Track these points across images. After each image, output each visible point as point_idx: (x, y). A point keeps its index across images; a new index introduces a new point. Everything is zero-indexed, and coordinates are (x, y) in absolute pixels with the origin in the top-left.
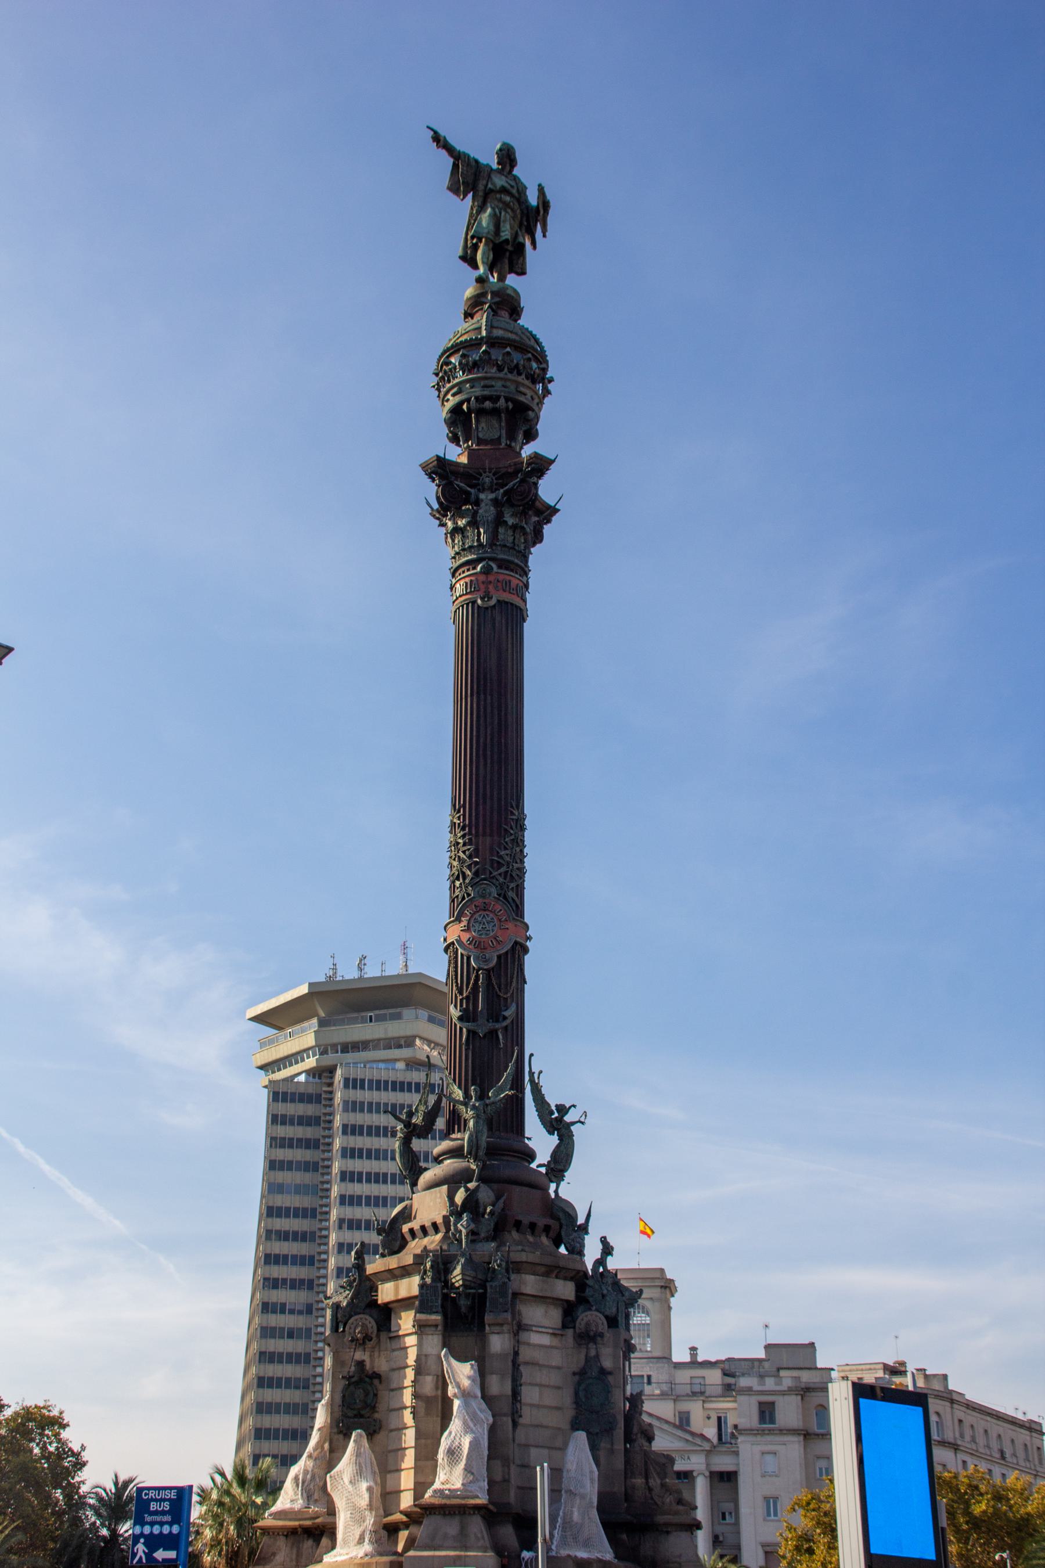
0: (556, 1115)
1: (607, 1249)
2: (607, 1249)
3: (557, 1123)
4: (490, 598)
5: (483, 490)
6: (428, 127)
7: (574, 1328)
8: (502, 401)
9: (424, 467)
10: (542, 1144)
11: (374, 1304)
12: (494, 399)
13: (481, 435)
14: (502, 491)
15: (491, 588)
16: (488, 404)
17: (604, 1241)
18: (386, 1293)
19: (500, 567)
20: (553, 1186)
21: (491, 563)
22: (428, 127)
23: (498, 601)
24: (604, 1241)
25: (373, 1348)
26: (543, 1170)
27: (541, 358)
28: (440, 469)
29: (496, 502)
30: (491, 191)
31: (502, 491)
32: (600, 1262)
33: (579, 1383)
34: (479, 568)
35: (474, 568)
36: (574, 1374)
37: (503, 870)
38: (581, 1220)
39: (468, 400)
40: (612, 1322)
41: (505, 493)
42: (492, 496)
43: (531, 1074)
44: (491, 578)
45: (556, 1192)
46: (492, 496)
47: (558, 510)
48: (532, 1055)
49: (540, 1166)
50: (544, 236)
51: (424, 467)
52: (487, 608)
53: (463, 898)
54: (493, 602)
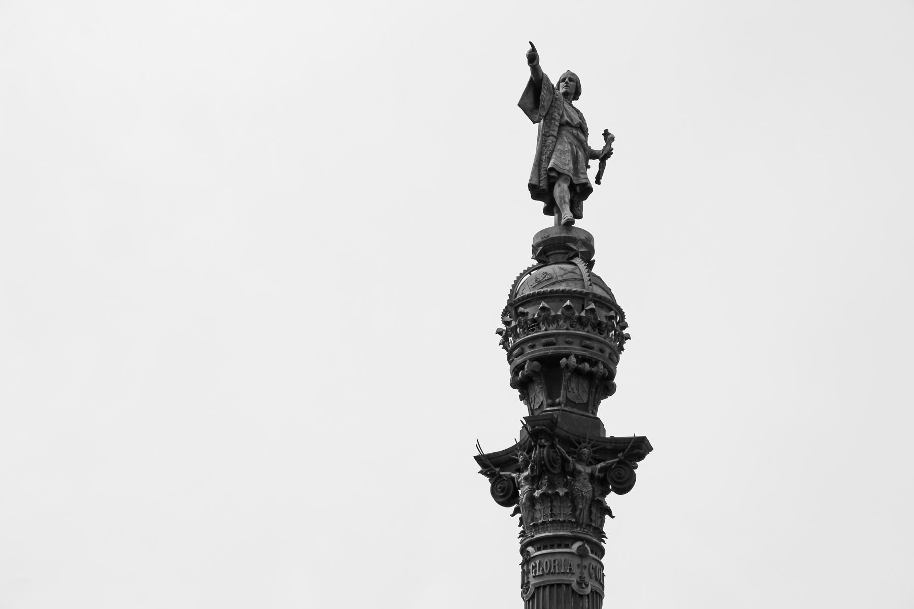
4: (587, 586)
5: (580, 460)
6: (531, 43)
12: (594, 363)
13: (570, 396)
15: (586, 574)
16: (587, 366)
19: (592, 552)
22: (531, 43)
29: (592, 476)
30: (568, 124)
31: (599, 466)
35: (567, 546)
41: (601, 470)
42: (589, 470)
44: (586, 563)
46: (589, 470)
50: (598, 181)
52: (581, 596)
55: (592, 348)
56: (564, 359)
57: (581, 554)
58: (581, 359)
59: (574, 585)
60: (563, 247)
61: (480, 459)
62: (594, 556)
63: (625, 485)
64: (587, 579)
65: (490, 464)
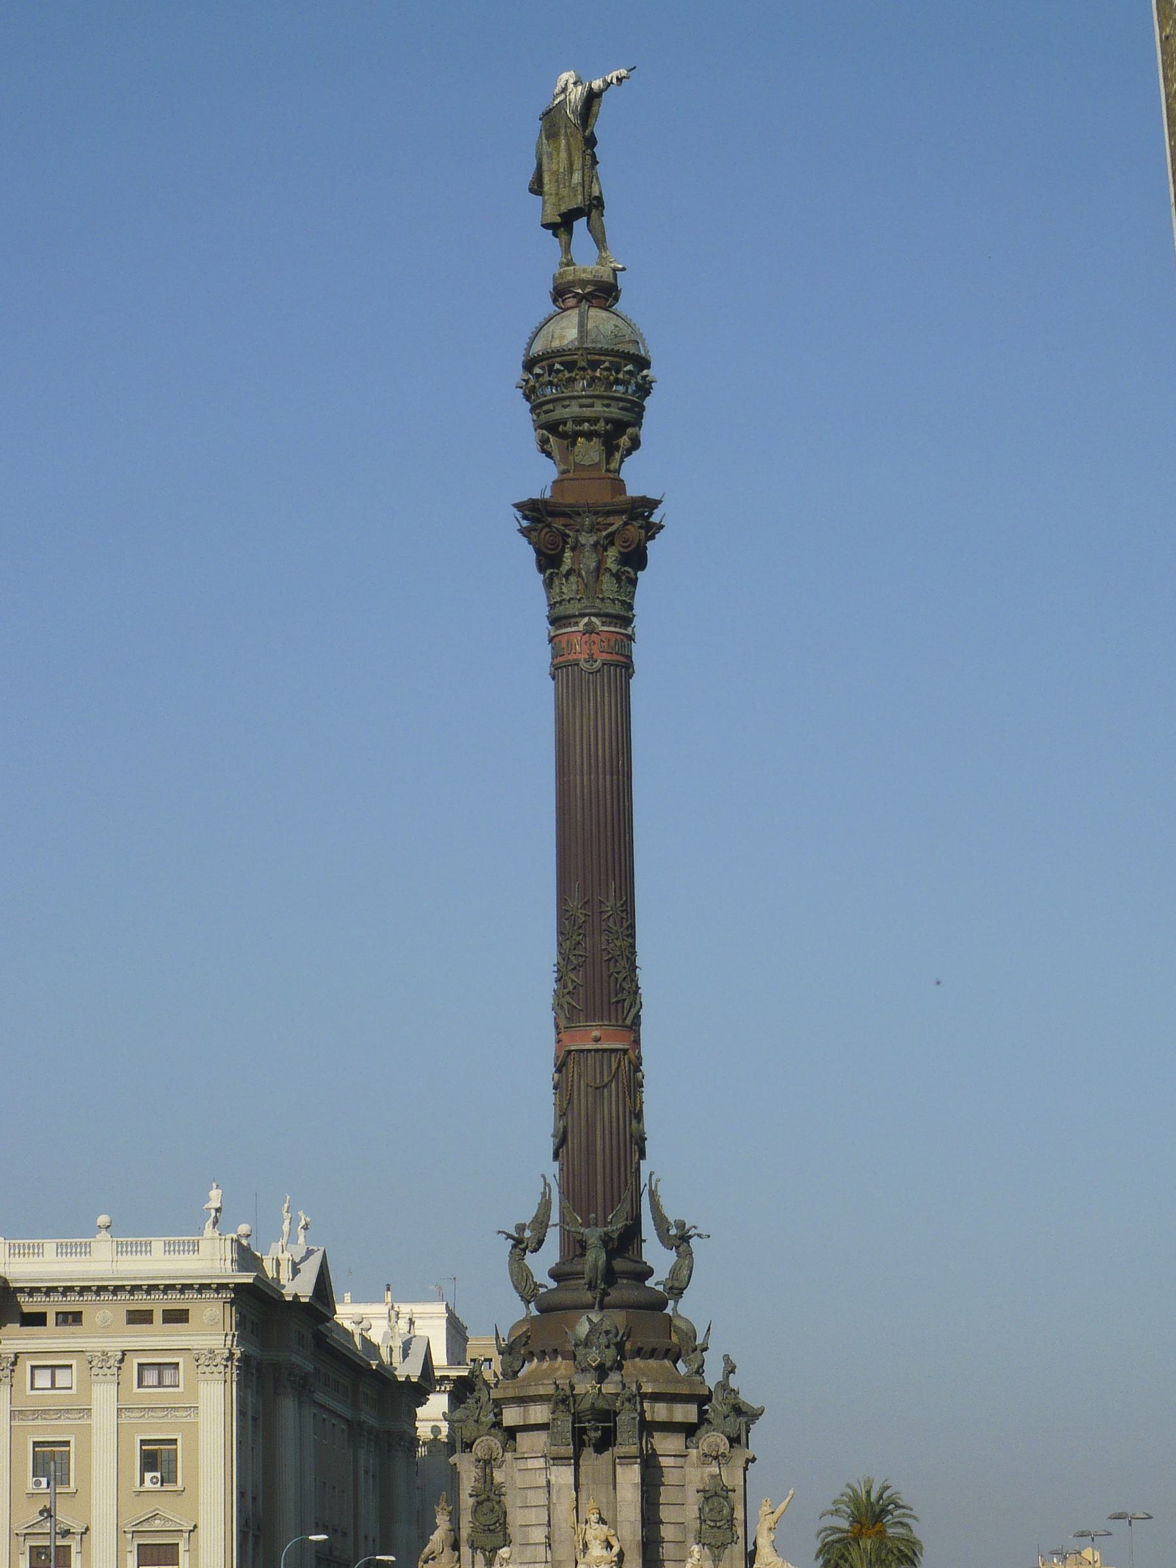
0: (673, 1231)
1: (731, 1369)
9: (519, 506)
11: (497, 1424)
17: (727, 1358)
18: (511, 1416)
19: (603, 624)
20: (671, 1303)
21: (593, 619)
23: (603, 664)
24: (727, 1358)
25: (500, 1467)
26: (660, 1288)
27: (643, 363)
28: (536, 514)
32: (724, 1386)
33: (707, 1499)
34: (581, 624)
38: (699, 1341)
40: (734, 1441)
45: (675, 1309)
47: (662, 527)
51: (519, 506)
54: (598, 664)
58: (579, 421)
59: (583, 664)
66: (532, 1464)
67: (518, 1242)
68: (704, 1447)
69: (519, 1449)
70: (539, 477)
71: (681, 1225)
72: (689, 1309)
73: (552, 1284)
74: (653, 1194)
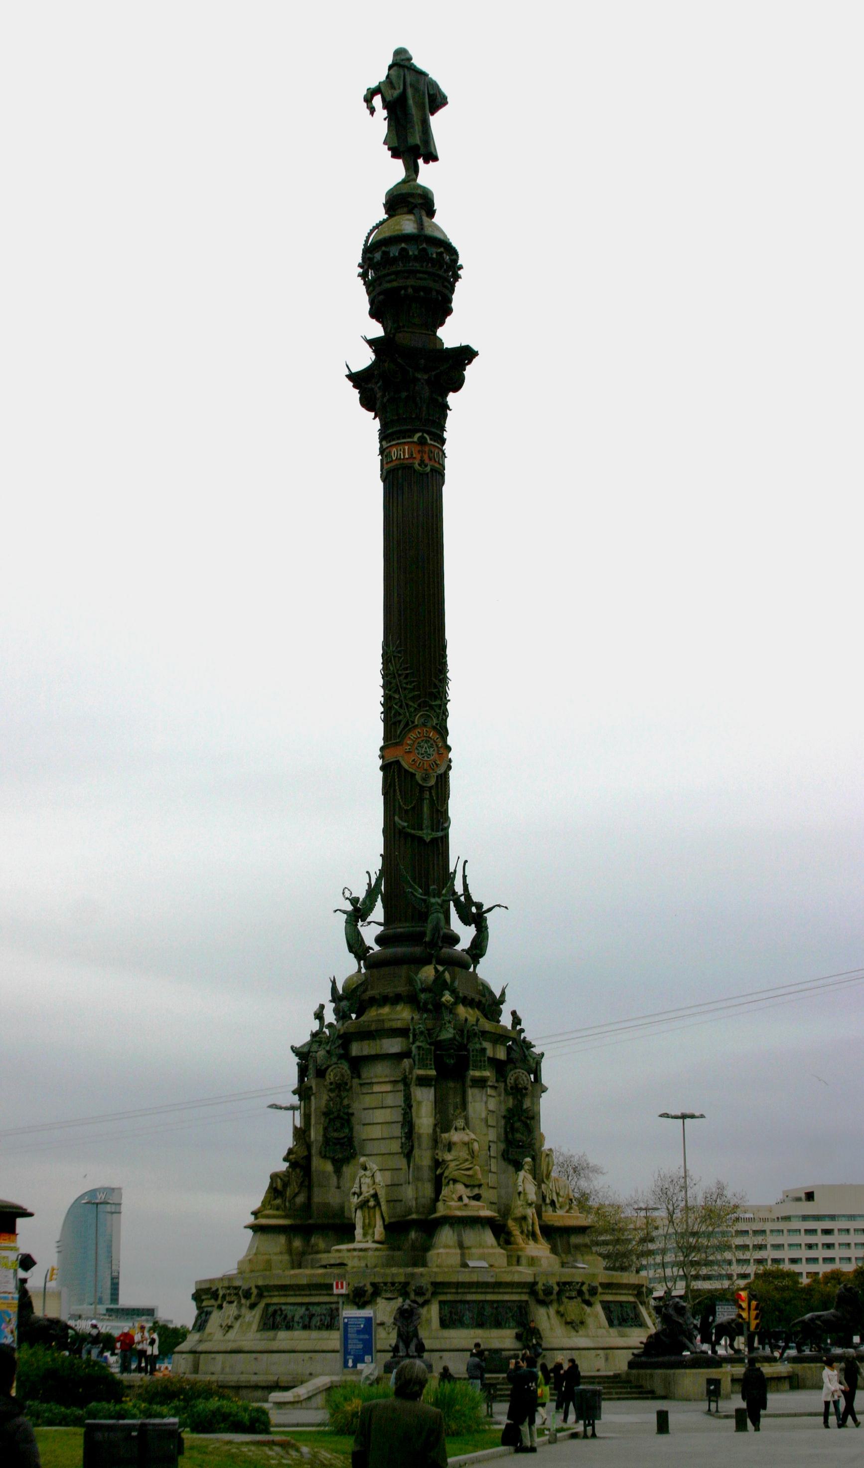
1: (516, 1020)
2: (516, 1020)
3: (475, 916)
4: (426, 466)
7: (505, 1082)
8: (434, 293)
10: (466, 934)
14: (433, 373)
15: (426, 457)
17: (514, 1013)
19: (431, 439)
21: (425, 435)
23: (432, 470)
24: (514, 1013)
29: (428, 382)
31: (433, 373)
34: (416, 438)
35: (410, 437)
36: (504, 1117)
37: (438, 702)
39: (406, 288)
42: (426, 377)
43: (465, 877)
46: (426, 377)
48: (466, 862)
49: (463, 950)
52: (421, 474)
53: (407, 724)
54: (428, 469)
55: (425, 279)
56: (403, 292)
57: (422, 442)
58: (416, 289)
59: (416, 466)
60: (409, 201)
61: (351, 377)
62: (432, 443)
63: (457, 384)
64: (427, 461)
65: (357, 379)
66: (376, 1088)
67: (356, 910)
68: (511, 1080)
69: (364, 1075)
70: (377, 330)
71: (479, 906)
72: (487, 970)
73: (377, 948)
74: (465, 877)
